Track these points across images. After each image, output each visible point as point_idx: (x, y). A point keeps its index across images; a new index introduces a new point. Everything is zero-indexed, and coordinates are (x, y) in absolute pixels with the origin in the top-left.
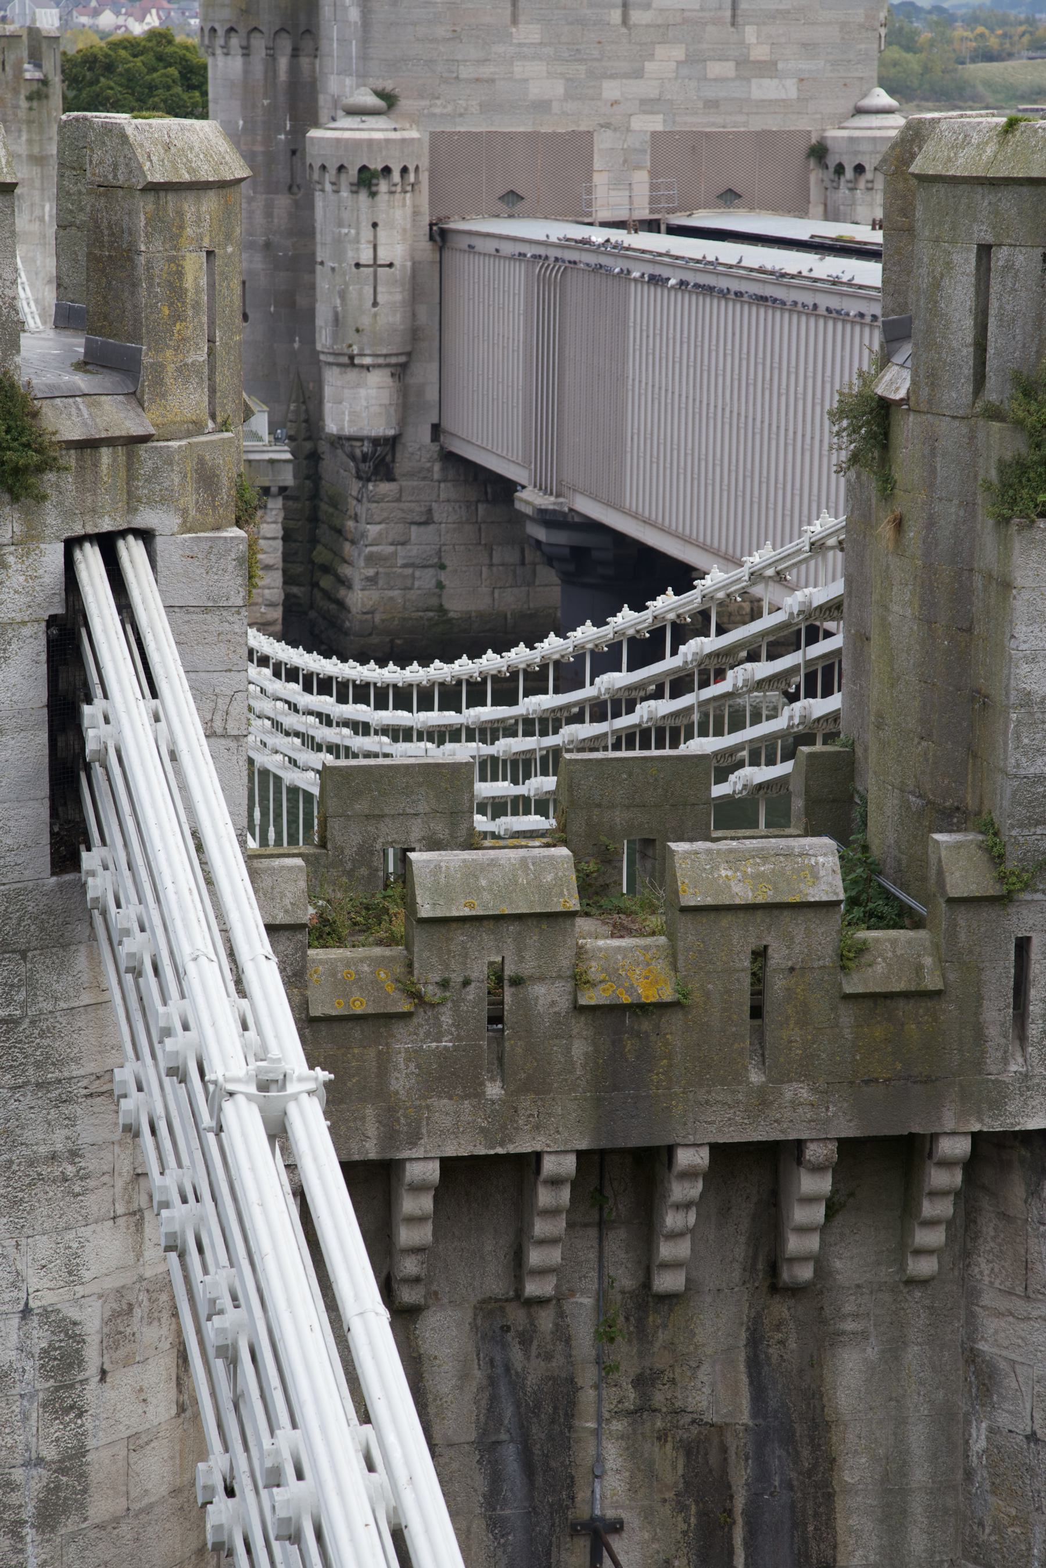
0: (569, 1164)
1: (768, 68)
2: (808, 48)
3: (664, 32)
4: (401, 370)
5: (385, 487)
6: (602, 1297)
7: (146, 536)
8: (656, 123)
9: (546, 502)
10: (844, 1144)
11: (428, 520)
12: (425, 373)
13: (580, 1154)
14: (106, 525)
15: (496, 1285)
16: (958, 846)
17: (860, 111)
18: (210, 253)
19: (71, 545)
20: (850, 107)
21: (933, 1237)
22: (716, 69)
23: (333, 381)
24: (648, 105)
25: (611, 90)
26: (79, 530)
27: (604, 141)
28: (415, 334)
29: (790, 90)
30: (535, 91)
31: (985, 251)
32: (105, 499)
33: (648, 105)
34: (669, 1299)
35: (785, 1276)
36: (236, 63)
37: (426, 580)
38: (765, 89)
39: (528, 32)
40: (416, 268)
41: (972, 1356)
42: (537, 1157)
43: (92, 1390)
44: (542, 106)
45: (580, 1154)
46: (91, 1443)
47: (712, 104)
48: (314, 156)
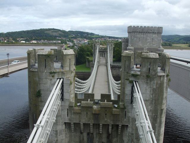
0: (92, 124)
1: (154, 45)
2: (157, 43)
3: (148, 42)
6: (96, 133)
7: (63, 78)
8: (147, 47)
10: (112, 125)
13: (93, 124)
14: (60, 77)
15: (89, 132)
16: (121, 104)
17: (159, 47)
18: (70, 59)
19: (58, 79)
20: (158, 47)
21: (120, 131)
22: (151, 44)
24: (147, 46)
25: (145, 45)
26: (58, 78)
27: (144, 48)
29: (155, 46)
31: (125, 61)
32: (60, 76)
33: (147, 46)
34: (101, 134)
35: (109, 133)
38: (154, 46)
39: (140, 42)
41: (123, 139)
42: (90, 124)
43: (58, 136)
44: (141, 46)
45: (93, 124)
46: (58, 139)
47: (151, 46)
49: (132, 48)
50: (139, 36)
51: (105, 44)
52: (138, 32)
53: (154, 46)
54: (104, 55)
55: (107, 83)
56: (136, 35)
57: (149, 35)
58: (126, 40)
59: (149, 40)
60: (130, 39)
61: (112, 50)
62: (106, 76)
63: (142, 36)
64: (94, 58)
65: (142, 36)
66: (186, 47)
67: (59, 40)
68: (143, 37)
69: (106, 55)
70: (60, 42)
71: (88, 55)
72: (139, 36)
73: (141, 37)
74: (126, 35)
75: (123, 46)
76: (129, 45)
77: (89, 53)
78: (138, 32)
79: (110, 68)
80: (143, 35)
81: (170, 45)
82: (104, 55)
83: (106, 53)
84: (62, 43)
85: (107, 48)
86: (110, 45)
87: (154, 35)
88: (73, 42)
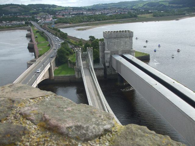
1: (127, 47)
4: (110, 63)
5: (109, 68)
9: (117, 72)
11: (111, 69)
12: (111, 63)
23: (106, 63)
28: (110, 61)
30: (116, 49)
36: (101, 47)
37: (111, 72)
38: (127, 48)
39: (115, 46)
40: (110, 57)
44: (116, 49)
48: (105, 53)
49: (109, 52)
50: (114, 41)
51: (72, 22)
52: (113, 37)
53: (127, 48)
54: (85, 60)
55: (98, 97)
56: (112, 40)
57: (122, 39)
58: (102, 40)
59: (123, 44)
60: (106, 44)
61: (92, 55)
62: (93, 83)
63: (117, 41)
64: (78, 63)
65: (117, 41)
66: (151, 17)
67: (22, 20)
68: (118, 41)
69: (87, 60)
70: (24, 23)
71: (67, 54)
72: (114, 41)
73: (116, 42)
74: (102, 37)
75: (100, 49)
76: (106, 48)
77: (68, 52)
78: (113, 37)
79: (94, 72)
80: (118, 40)
81: (135, 16)
82: (85, 60)
83: (87, 58)
84: (27, 24)
85: (87, 54)
86: (90, 51)
87: (126, 39)
88: (37, 21)
